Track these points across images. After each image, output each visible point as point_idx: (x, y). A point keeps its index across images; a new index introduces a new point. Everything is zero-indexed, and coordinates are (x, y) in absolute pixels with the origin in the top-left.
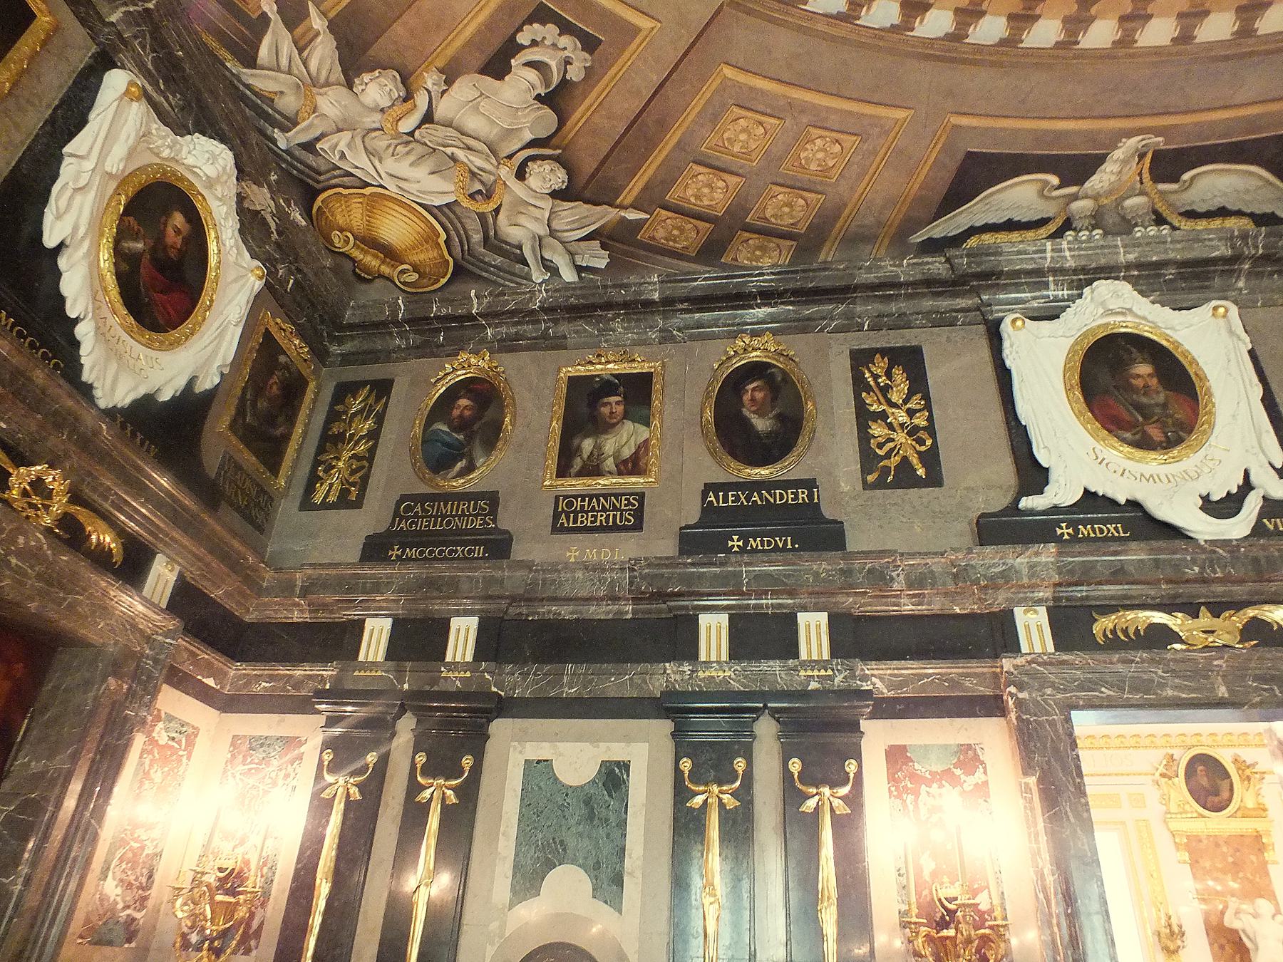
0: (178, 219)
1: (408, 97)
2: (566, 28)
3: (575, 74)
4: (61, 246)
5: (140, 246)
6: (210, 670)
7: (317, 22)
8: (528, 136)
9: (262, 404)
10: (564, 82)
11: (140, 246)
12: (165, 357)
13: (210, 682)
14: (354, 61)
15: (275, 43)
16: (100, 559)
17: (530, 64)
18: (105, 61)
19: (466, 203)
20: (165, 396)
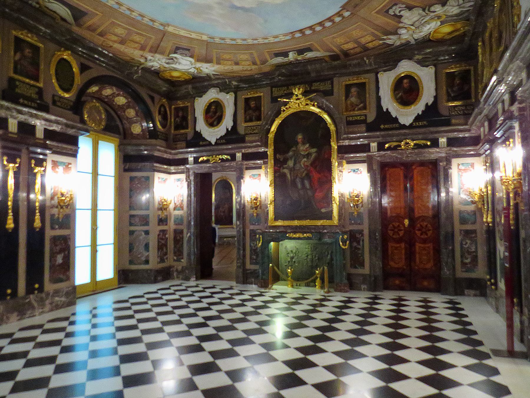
0: (405, 81)
1: (406, 28)
2: (391, 8)
3: (404, 6)
4: (387, 109)
5: (400, 94)
6: (470, 150)
7: (385, 37)
8: (421, 11)
9: (455, 89)
10: (405, 7)
11: (400, 94)
12: (417, 106)
13: (472, 153)
14: (395, 33)
15: (388, 42)
16: (426, 146)
17: (400, 12)
18: (377, 73)
19: (441, 20)
20: (420, 113)
